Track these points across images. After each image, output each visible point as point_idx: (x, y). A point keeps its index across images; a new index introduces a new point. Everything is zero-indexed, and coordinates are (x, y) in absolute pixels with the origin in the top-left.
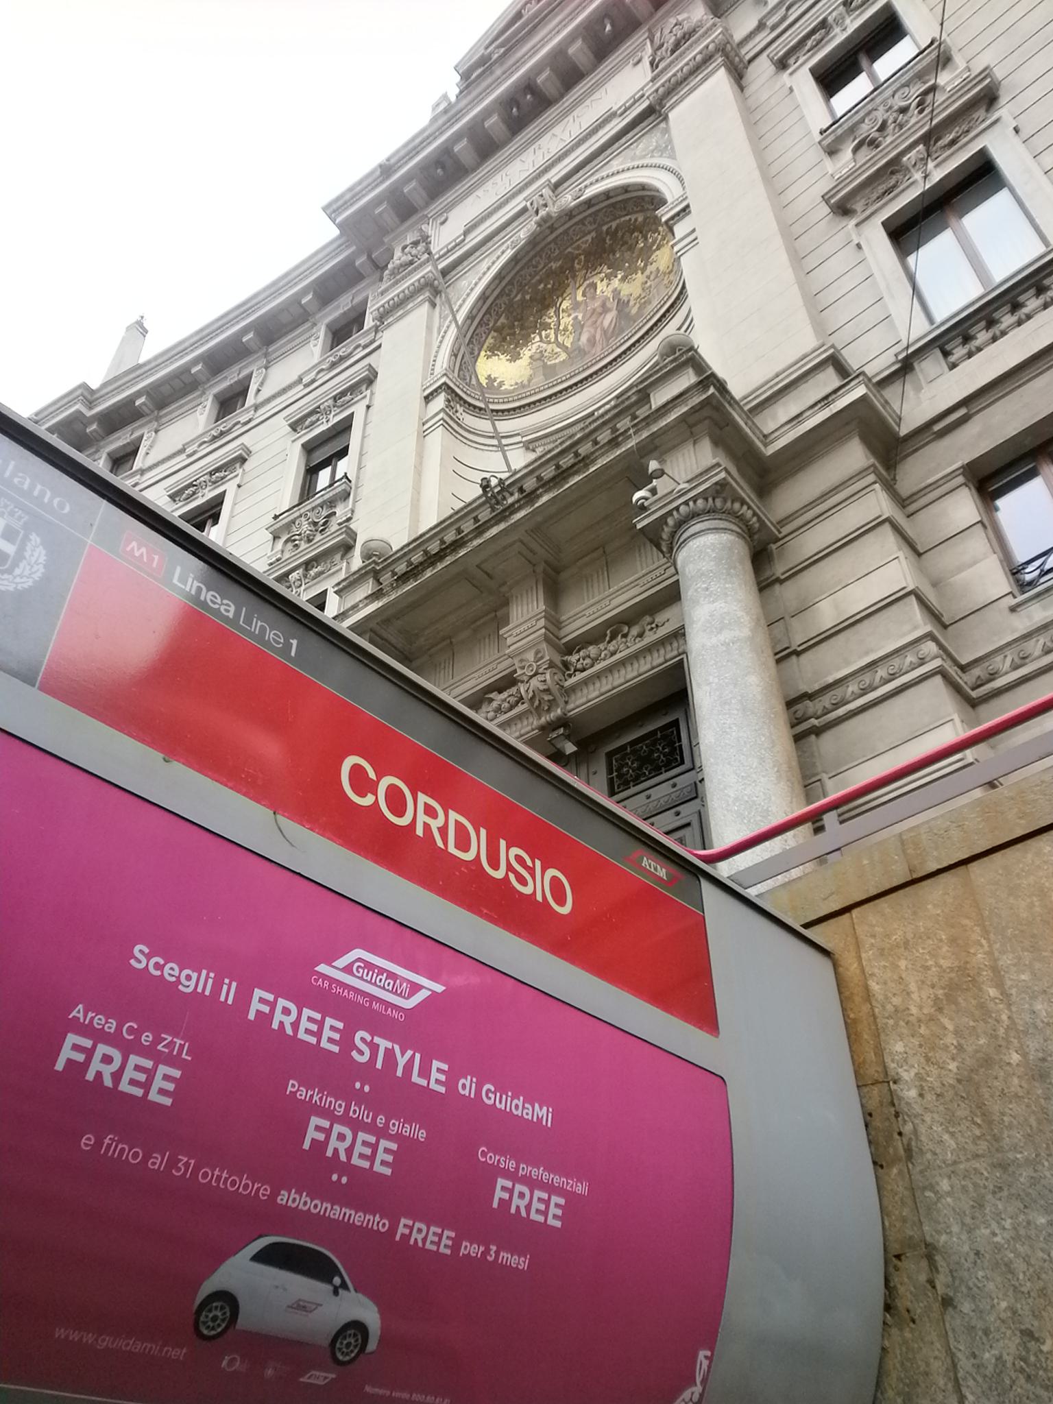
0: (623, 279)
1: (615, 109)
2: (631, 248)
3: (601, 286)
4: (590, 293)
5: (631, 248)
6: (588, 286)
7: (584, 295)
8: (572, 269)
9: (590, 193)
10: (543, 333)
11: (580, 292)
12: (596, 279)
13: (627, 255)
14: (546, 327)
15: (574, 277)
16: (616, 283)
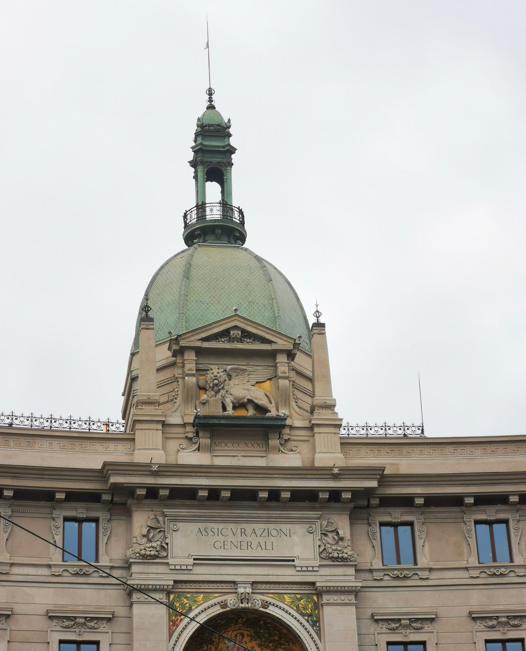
0: (260, 646)
1: (296, 563)
2: (270, 635)
3: (246, 639)
4: (239, 637)
5: (270, 635)
6: (240, 633)
7: (236, 636)
8: (237, 621)
9: (272, 610)
10: (209, 645)
11: (234, 633)
12: (245, 633)
13: (266, 635)
14: (212, 642)
15: (236, 624)
16: (254, 643)
